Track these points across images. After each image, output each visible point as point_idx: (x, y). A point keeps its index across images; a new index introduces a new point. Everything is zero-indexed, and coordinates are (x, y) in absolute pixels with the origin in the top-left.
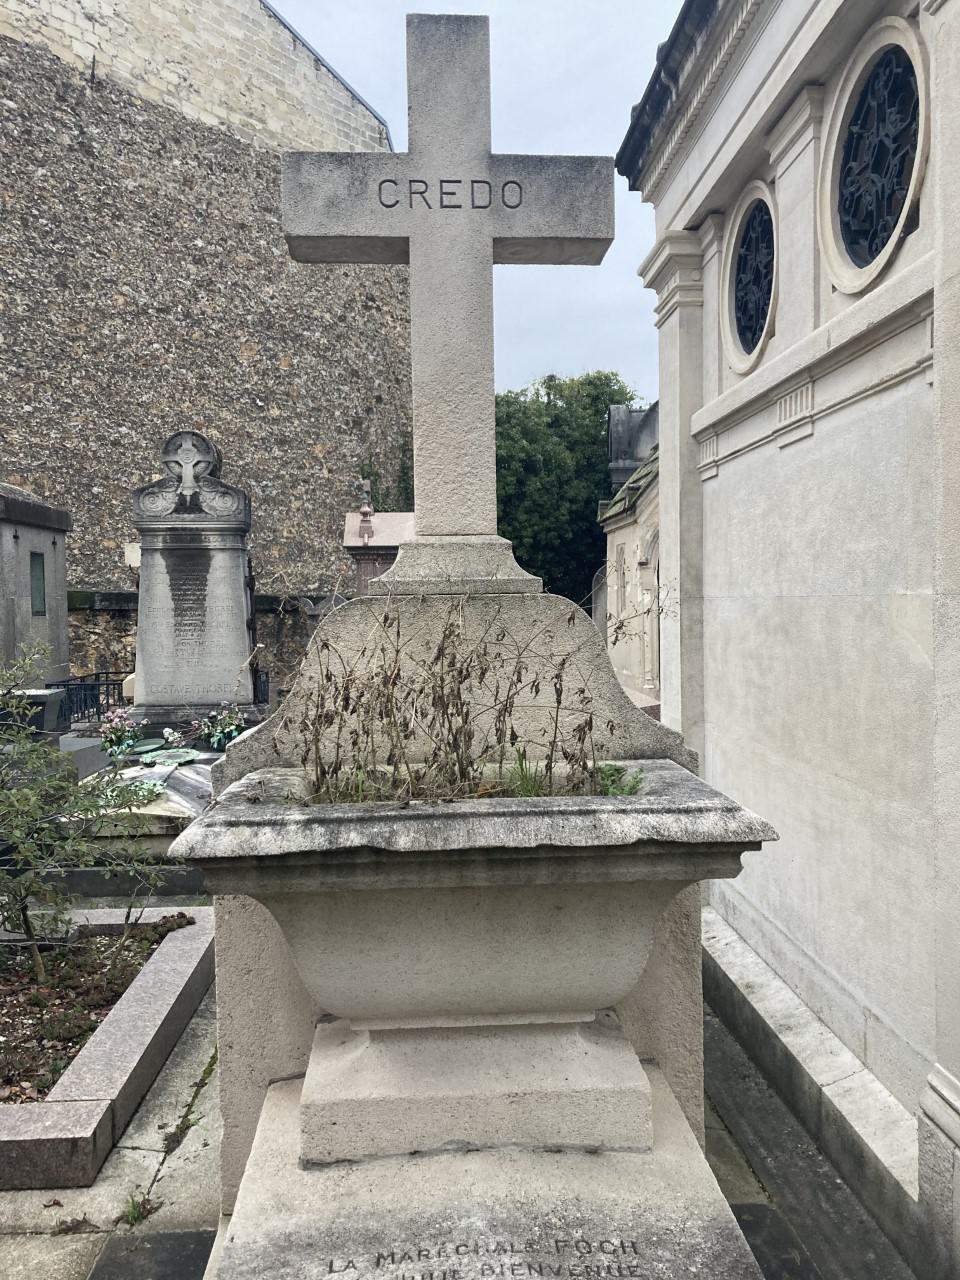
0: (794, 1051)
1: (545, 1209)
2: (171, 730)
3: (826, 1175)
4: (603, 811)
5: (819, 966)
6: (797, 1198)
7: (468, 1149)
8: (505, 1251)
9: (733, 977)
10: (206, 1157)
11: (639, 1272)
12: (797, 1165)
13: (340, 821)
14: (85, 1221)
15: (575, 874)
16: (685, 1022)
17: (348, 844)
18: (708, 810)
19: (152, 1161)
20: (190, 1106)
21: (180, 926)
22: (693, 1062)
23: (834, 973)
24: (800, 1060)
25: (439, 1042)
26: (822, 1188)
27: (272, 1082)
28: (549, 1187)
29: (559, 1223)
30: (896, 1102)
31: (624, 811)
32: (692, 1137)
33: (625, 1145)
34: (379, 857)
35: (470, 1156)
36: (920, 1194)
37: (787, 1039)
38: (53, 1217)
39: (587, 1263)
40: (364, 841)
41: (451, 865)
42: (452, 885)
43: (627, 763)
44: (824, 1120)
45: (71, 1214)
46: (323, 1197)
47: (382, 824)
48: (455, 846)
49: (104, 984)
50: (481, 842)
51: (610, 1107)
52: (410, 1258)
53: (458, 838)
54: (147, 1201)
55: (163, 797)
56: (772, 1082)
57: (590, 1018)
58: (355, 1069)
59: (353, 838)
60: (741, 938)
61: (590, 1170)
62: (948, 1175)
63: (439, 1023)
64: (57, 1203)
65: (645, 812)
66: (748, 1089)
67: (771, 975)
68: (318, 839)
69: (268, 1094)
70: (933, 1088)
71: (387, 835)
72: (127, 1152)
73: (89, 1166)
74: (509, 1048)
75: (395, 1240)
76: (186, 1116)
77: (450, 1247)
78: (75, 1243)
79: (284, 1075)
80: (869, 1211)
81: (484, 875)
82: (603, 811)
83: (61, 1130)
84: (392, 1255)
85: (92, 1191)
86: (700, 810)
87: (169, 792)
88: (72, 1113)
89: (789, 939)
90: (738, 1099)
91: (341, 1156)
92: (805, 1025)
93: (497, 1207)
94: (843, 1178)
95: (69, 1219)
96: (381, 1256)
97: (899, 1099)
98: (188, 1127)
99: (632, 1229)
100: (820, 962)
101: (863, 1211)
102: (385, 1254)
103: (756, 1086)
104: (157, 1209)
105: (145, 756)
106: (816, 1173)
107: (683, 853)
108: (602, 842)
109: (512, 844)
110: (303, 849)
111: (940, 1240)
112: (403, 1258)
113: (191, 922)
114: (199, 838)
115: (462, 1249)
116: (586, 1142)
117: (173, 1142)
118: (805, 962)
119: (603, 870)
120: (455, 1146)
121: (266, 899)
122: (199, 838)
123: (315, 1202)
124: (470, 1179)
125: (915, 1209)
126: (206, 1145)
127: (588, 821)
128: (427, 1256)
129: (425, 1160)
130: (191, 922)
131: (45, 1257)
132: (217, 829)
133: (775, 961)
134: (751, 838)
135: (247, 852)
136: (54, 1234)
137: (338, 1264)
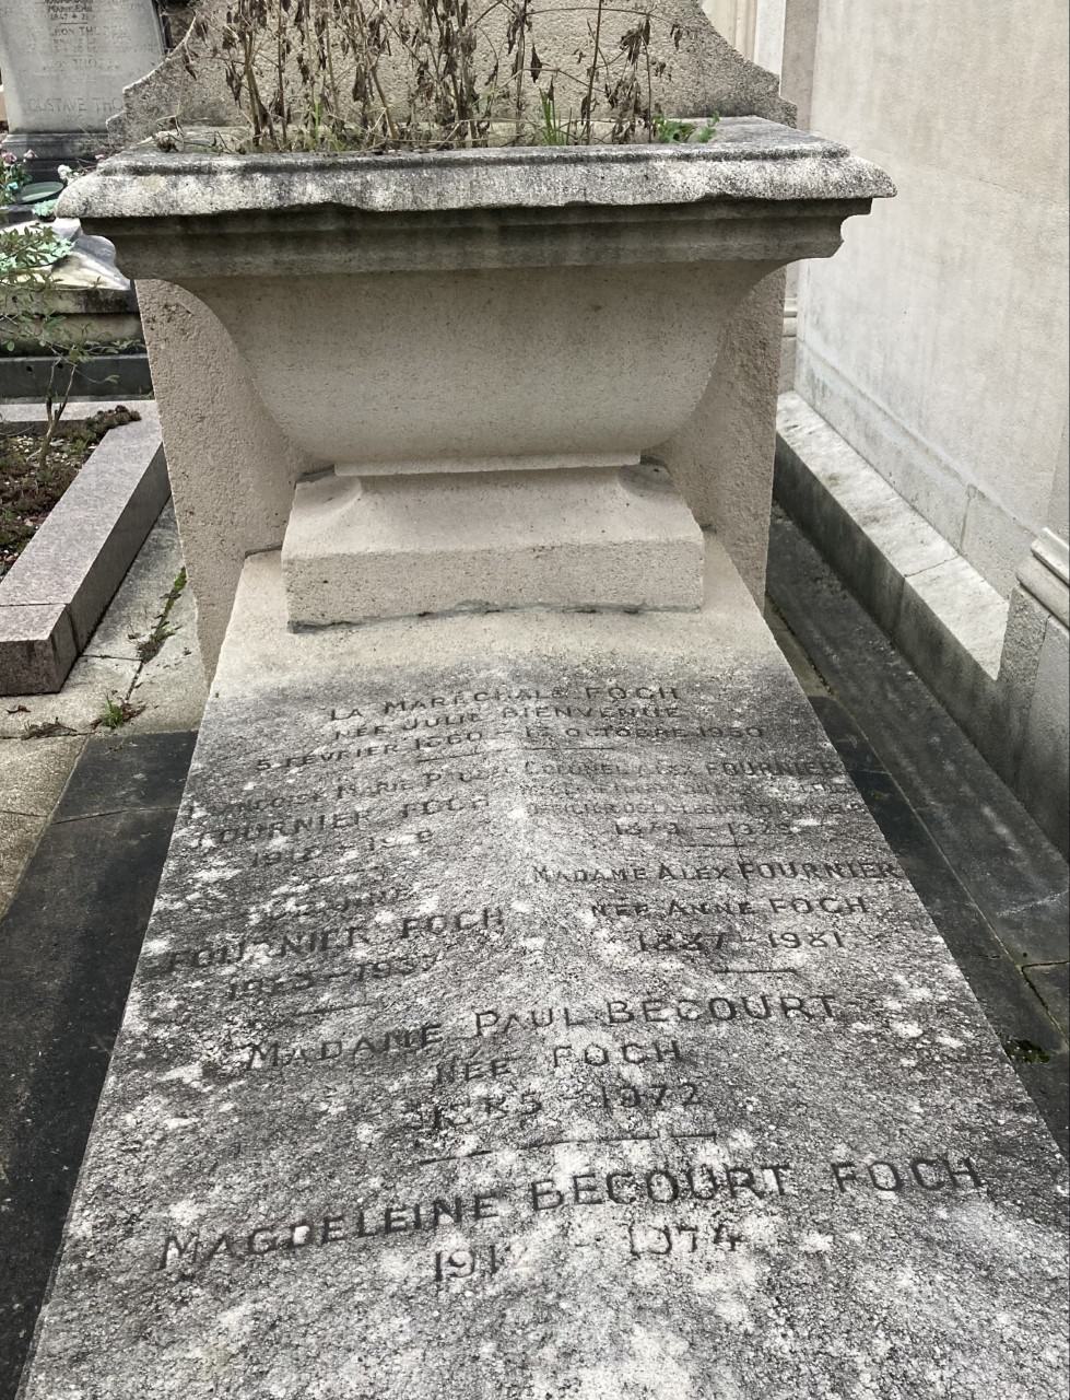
0: (877, 543)
1: (576, 662)
2: (68, 169)
3: (896, 668)
4: (659, 158)
5: (922, 444)
6: (861, 689)
7: (486, 609)
8: (530, 697)
9: (813, 469)
10: (189, 663)
11: (678, 713)
12: (864, 660)
13: (291, 169)
14: (58, 726)
15: (617, 250)
16: (755, 511)
17: (305, 200)
18: (804, 155)
19: (128, 670)
20: (163, 617)
21: (122, 423)
22: (757, 528)
23: (938, 449)
24: (884, 552)
25: (447, 493)
26: (891, 680)
27: (248, 554)
28: (579, 643)
29: (590, 674)
30: (989, 586)
31: (687, 157)
32: (749, 599)
33: (671, 603)
34: (351, 222)
35: (489, 616)
36: (1000, 672)
37: (873, 533)
38: (20, 723)
39: (620, 706)
40: (327, 197)
41: (450, 236)
42: (452, 267)
43: (698, 120)
44: (902, 612)
45: (40, 718)
46: (320, 657)
47: (351, 174)
48: (453, 205)
49: (36, 486)
50: (489, 199)
51: (654, 563)
52: (422, 705)
53: (456, 193)
54: (125, 707)
55: (73, 261)
56: (848, 582)
57: (634, 461)
58: (347, 523)
59: (311, 192)
60: (830, 425)
61: (628, 628)
62: (1036, 647)
63: (447, 468)
64: (23, 709)
65: (717, 158)
66: (819, 592)
67: (861, 464)
68: (262, 193)
69: (246, 566)
70: (1036, 556)
71: (359, 188)
72: (96, 660)
73: (53, 670)
74: (532, 499)
75: (404, 691)
76: (159, 628)
77: (467, 695)
78: (55, 744)
79: (263, 547)
80: (939, 698)
81: (495, 252)
82: (659, 158)
83: (11, 634)
84: (403, 704)
85: (61, 697)
86: (793, 155)
87: (82, 256)
88: (21, 617)
89: (890, 417)
90: (807, 602)
91: (337, 618)
92: (896, 516)
93: (521, 661)
94: (915, 670)
95: (40, 724)
96: (389, 705)
97: (991, 584)
98: (164, 637)
99: (673, 677)
100: (923, 439)
101: (932, 699)
102: (394, 703)
103: (829, 588)
104: (139, 713)
105: (38, 205)
106: (886, 667)
107: (765, 220)
108: (656, 200)
109: (532, 202)
110: (242, 206)
111: (1015, 715)
112: (413, 707)
113: (135, 418)
114: (95, 189)
115: (481, 697)
116: (625, 601)
117: (148, 652)
118: (903, 442)
119: (656, 244)
120: (471, 607)
121: (203, 291)
122: (95, 189)
123: (311, 660)
124: (489, 637)
125: (992, 688)
126: (187, 653)
127: (639, 170)
128: (442, 703)
129: (438, 622)
130: (135, 418)
131: (17, 758)
132: (119, 178)
133: (868, 448)
134: (859, 193)
135: (166, 210)
136: (25, 738)
137: (340, 713)
